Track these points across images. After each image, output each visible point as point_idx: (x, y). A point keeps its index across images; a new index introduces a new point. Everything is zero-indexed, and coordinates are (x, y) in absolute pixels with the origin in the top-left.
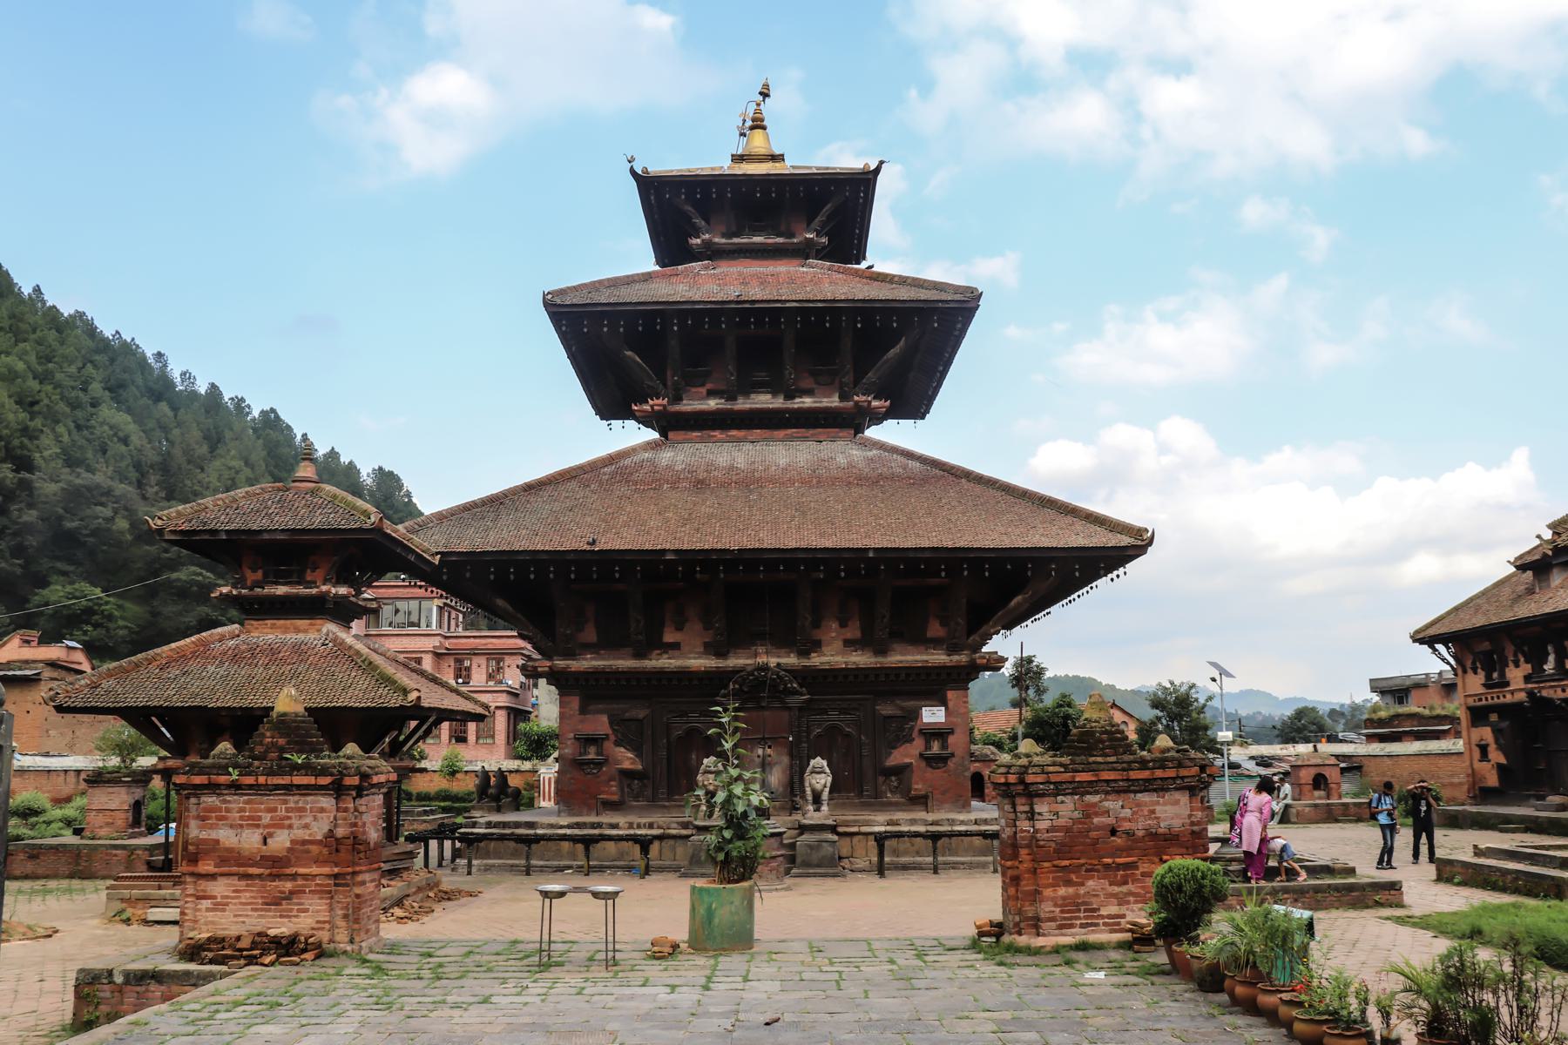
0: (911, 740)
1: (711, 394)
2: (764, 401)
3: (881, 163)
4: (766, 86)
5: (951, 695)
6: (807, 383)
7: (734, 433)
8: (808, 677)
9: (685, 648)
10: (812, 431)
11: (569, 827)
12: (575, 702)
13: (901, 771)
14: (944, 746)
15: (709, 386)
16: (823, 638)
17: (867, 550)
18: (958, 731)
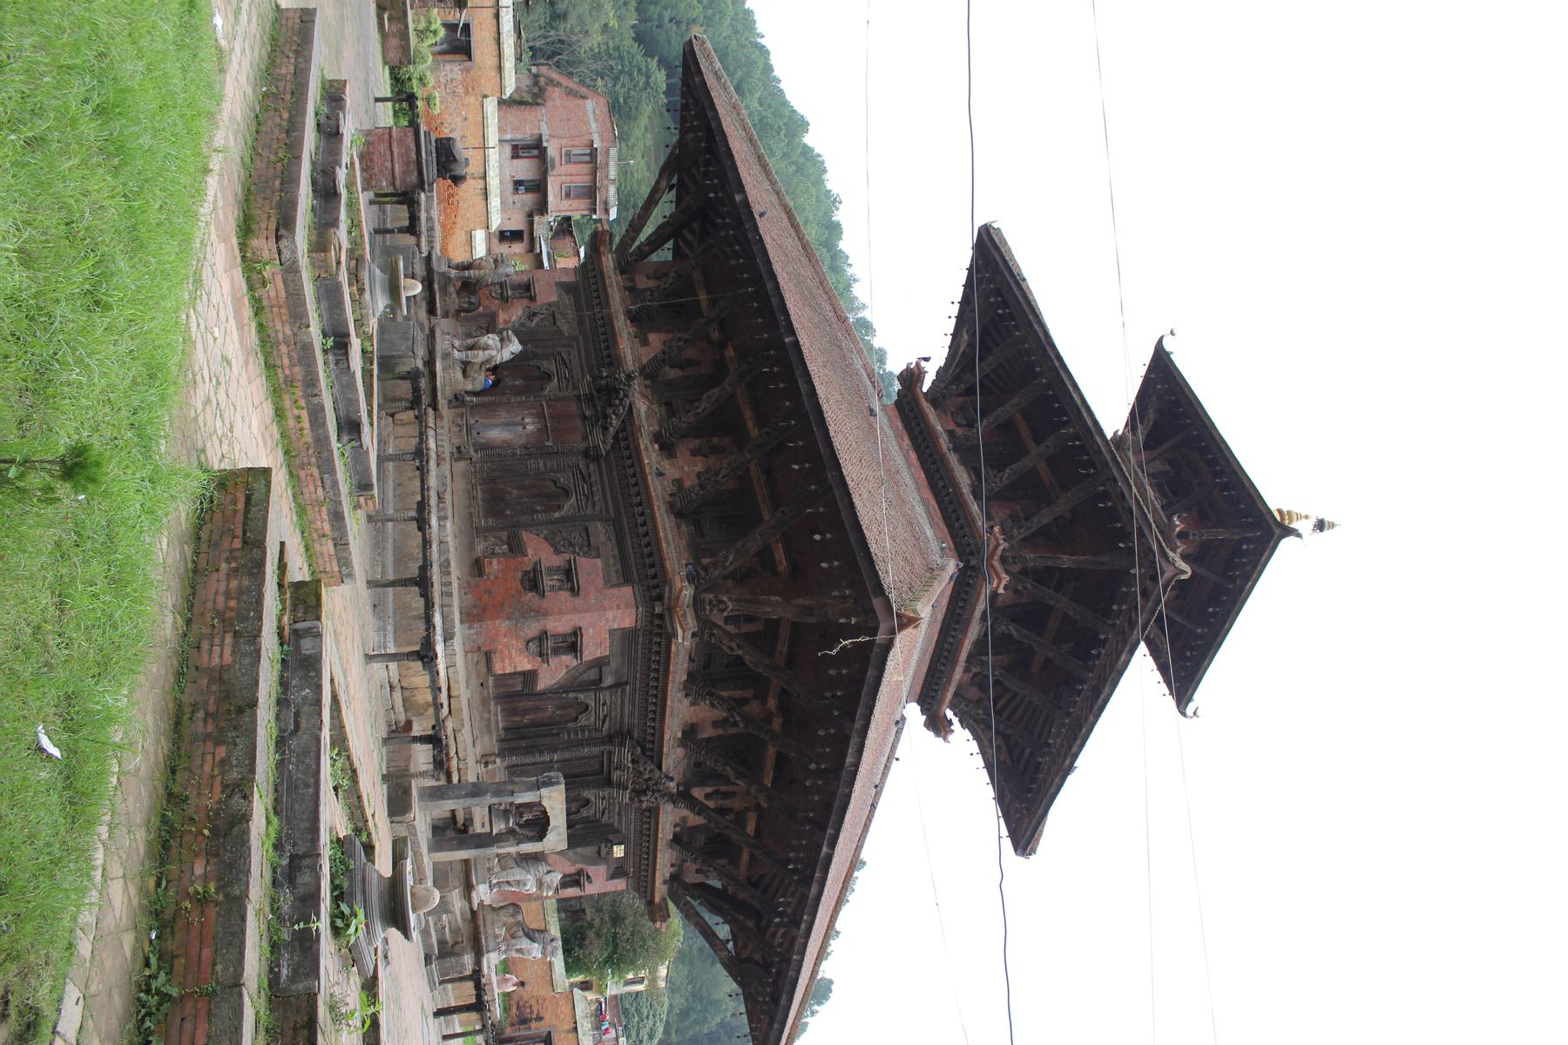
0: (557, 552)
1: (951, 434)
2: (963, 478)
3: (1299, 536)
4: (1332, 525)
5: (627, 591)
6: (999, 515)
7: (913, 455)
8: (625, 439)
9: (643, 350)
10: (941, 522)
11: (429, 219)
12: (571, 278)
13: (515, 547)
14: (552, 588)
15: (959, 431)
16: (680, 461)
17: (792, 332)
18: (578, 601)
